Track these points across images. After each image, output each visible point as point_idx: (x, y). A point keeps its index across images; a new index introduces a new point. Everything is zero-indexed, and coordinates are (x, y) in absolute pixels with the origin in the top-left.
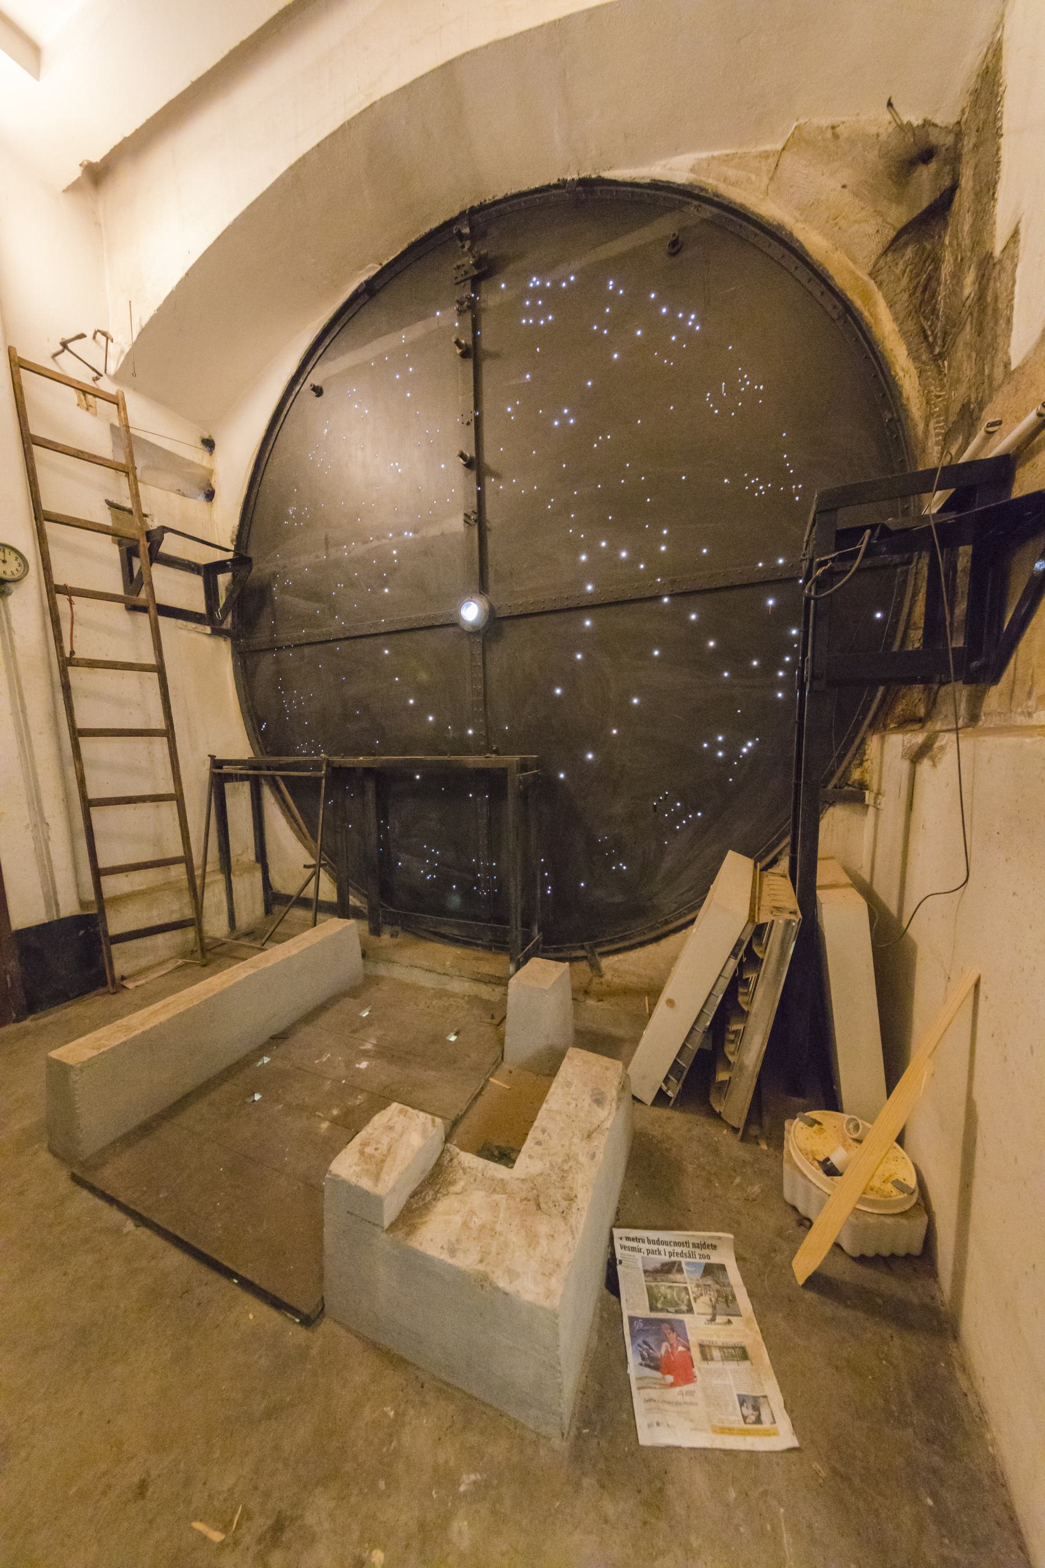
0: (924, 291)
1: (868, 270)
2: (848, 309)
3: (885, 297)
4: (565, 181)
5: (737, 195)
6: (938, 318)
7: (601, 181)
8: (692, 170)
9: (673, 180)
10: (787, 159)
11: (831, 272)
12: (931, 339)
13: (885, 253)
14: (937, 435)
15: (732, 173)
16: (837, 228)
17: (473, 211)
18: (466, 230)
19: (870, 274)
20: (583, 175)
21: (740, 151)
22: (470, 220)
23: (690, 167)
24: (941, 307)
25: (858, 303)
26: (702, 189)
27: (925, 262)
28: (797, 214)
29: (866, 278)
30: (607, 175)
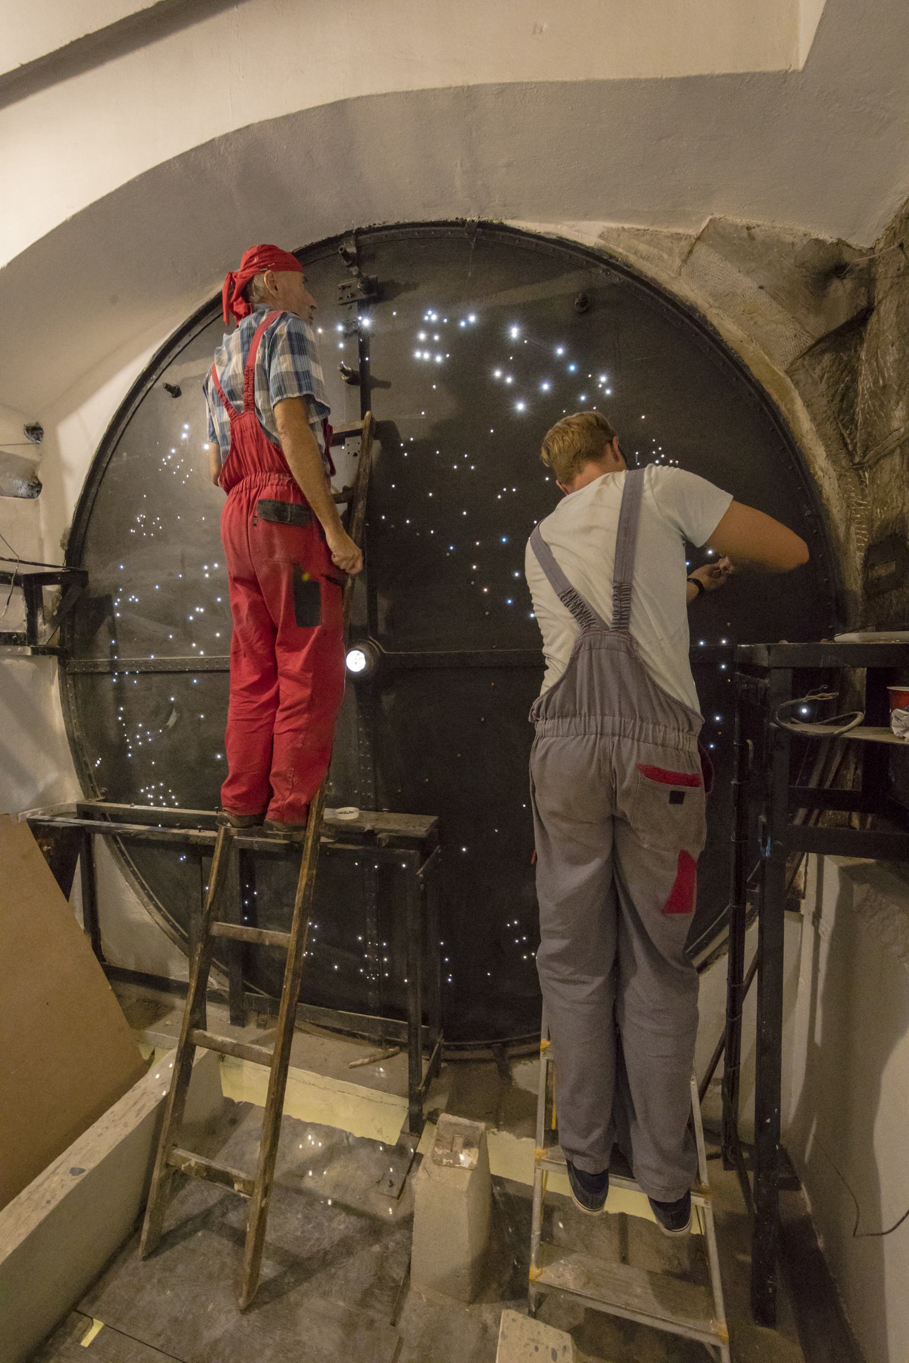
0: (842, 400)
1: (785, 367)
2: (764, 397)
3: (802, 395)
4: (464, 222)
5: (650, 270)
6: (856, 428)
7: (502, 227)
8: (601, 236)
9: (579, 240)
10: (702, 250)
11: (747, 362)
12: (850, 447)
13: (803, 356)
14: (859, 540)
15: (642, 247)
16: (752, 323)
17: (360, 232)
18: (352, 250)
19: (786, 372)
20: (484, 219)
21: (651, 229)
22: (356, 241)
23: (599, 233)
24: (860, 418)
25: (775, 397)
26: (611, 257)
27: (843, 371)
28: (710, 300)
29: (782, 374)
30: (510, 223)
